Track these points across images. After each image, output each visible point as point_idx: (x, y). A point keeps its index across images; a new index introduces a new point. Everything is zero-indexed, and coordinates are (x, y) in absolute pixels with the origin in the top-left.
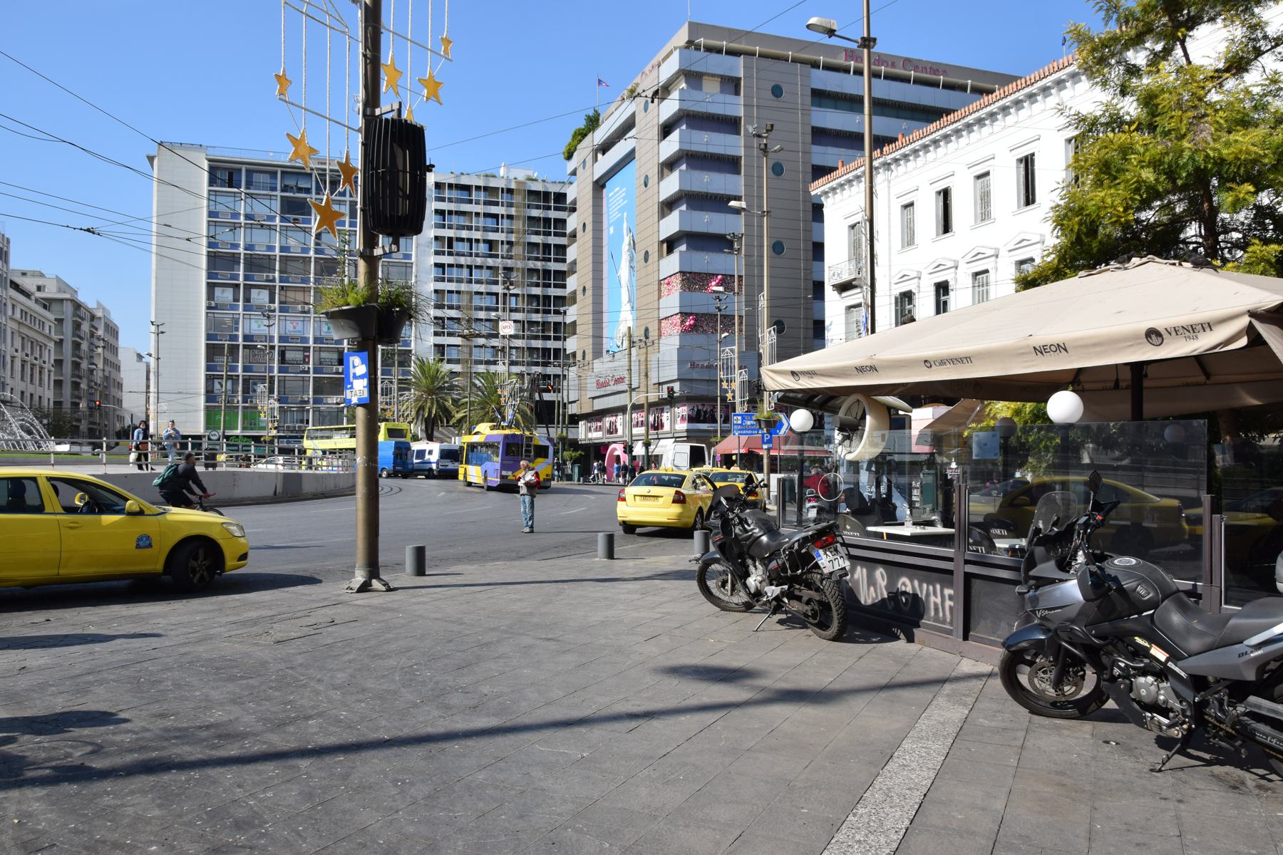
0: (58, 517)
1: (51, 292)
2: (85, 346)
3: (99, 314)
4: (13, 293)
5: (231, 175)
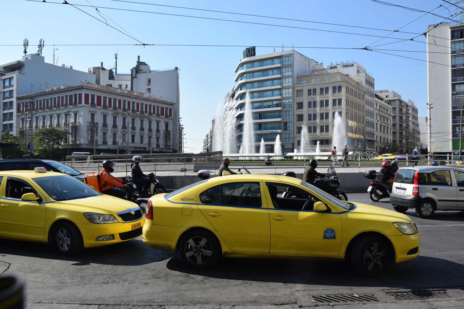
0: (270, 211)
1: (391, 98)
2: (404, 117)
3: (410, 104)
4: (376, 99)
5: (461, 33)
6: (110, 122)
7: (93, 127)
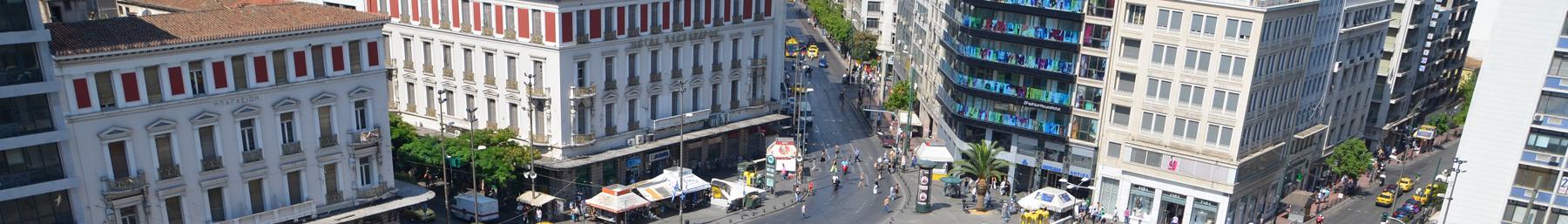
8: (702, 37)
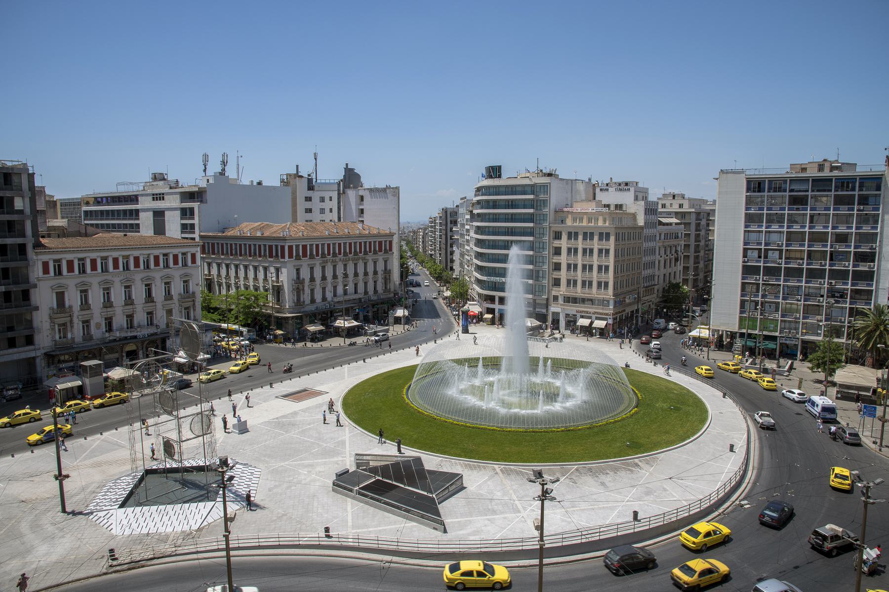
6: (318, 274)
7: (298, 284)
8: (358, 259)
